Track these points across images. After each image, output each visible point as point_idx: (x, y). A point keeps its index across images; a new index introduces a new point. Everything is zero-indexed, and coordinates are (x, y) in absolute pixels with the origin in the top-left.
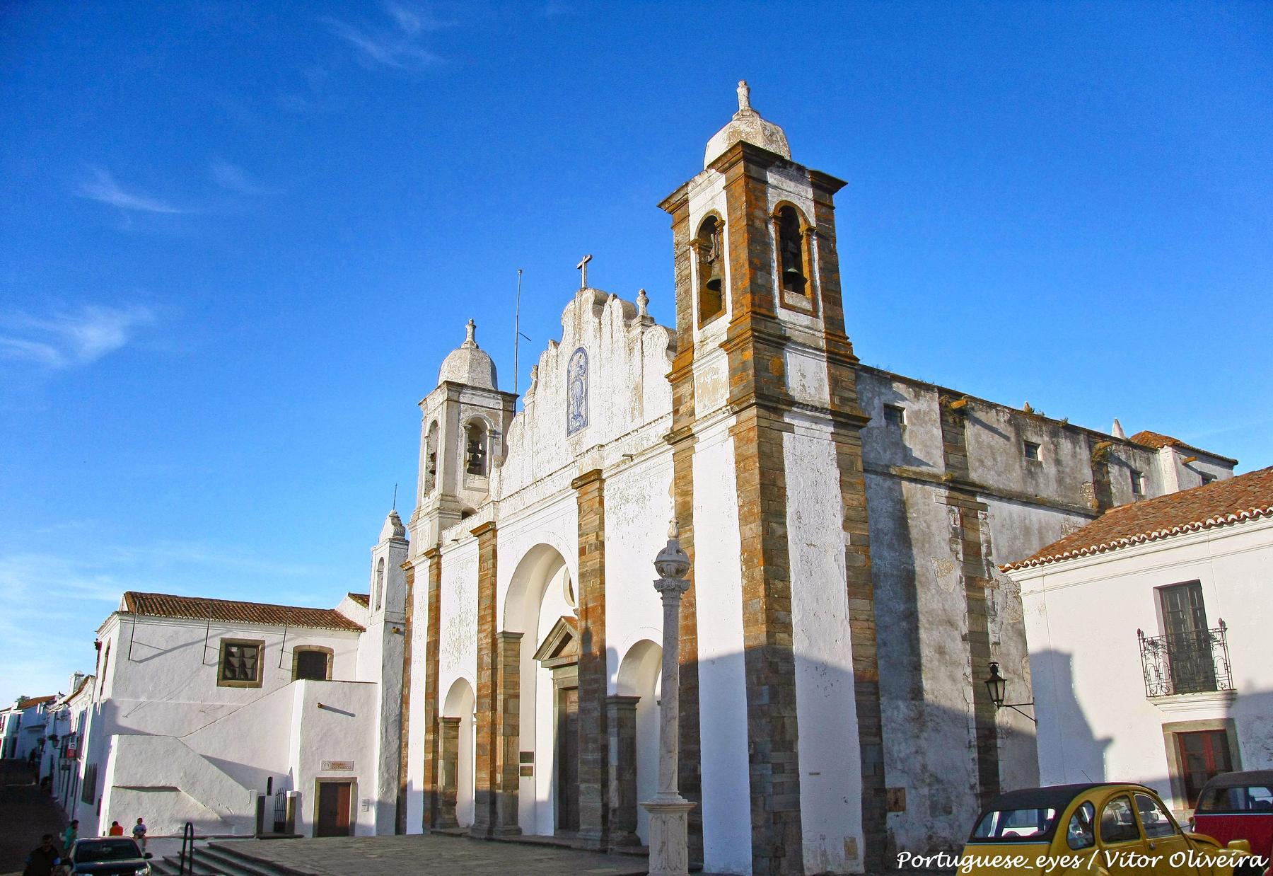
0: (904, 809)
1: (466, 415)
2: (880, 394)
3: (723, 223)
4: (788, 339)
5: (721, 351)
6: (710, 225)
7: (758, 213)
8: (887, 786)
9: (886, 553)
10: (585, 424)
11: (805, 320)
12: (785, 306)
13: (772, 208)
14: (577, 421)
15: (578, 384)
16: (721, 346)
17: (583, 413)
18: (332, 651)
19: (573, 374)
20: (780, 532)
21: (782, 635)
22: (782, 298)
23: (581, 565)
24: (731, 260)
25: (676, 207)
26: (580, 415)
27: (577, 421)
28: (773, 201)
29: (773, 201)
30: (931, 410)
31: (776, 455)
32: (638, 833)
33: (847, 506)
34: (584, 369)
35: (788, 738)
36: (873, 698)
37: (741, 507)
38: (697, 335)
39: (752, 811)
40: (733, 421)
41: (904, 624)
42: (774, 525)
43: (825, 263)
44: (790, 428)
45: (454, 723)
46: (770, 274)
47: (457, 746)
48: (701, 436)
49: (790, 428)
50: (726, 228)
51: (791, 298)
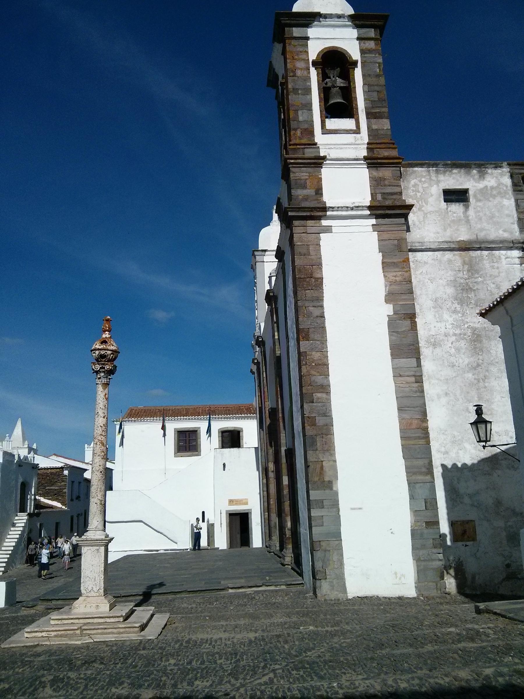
2: (438, 182)
4: (324, 158)
11: (350, 138)
12: (325, 131)
13: (313, 55)
21: (319, 395)
29: (314, 50)
30: (500, 184)
33: (389, 283)
35: (327, 479)
36: (422, 442)
42: (310, 308)
43: (369, 85)
44: (328, 230)
46: (310, 109)
51: (332, 123)
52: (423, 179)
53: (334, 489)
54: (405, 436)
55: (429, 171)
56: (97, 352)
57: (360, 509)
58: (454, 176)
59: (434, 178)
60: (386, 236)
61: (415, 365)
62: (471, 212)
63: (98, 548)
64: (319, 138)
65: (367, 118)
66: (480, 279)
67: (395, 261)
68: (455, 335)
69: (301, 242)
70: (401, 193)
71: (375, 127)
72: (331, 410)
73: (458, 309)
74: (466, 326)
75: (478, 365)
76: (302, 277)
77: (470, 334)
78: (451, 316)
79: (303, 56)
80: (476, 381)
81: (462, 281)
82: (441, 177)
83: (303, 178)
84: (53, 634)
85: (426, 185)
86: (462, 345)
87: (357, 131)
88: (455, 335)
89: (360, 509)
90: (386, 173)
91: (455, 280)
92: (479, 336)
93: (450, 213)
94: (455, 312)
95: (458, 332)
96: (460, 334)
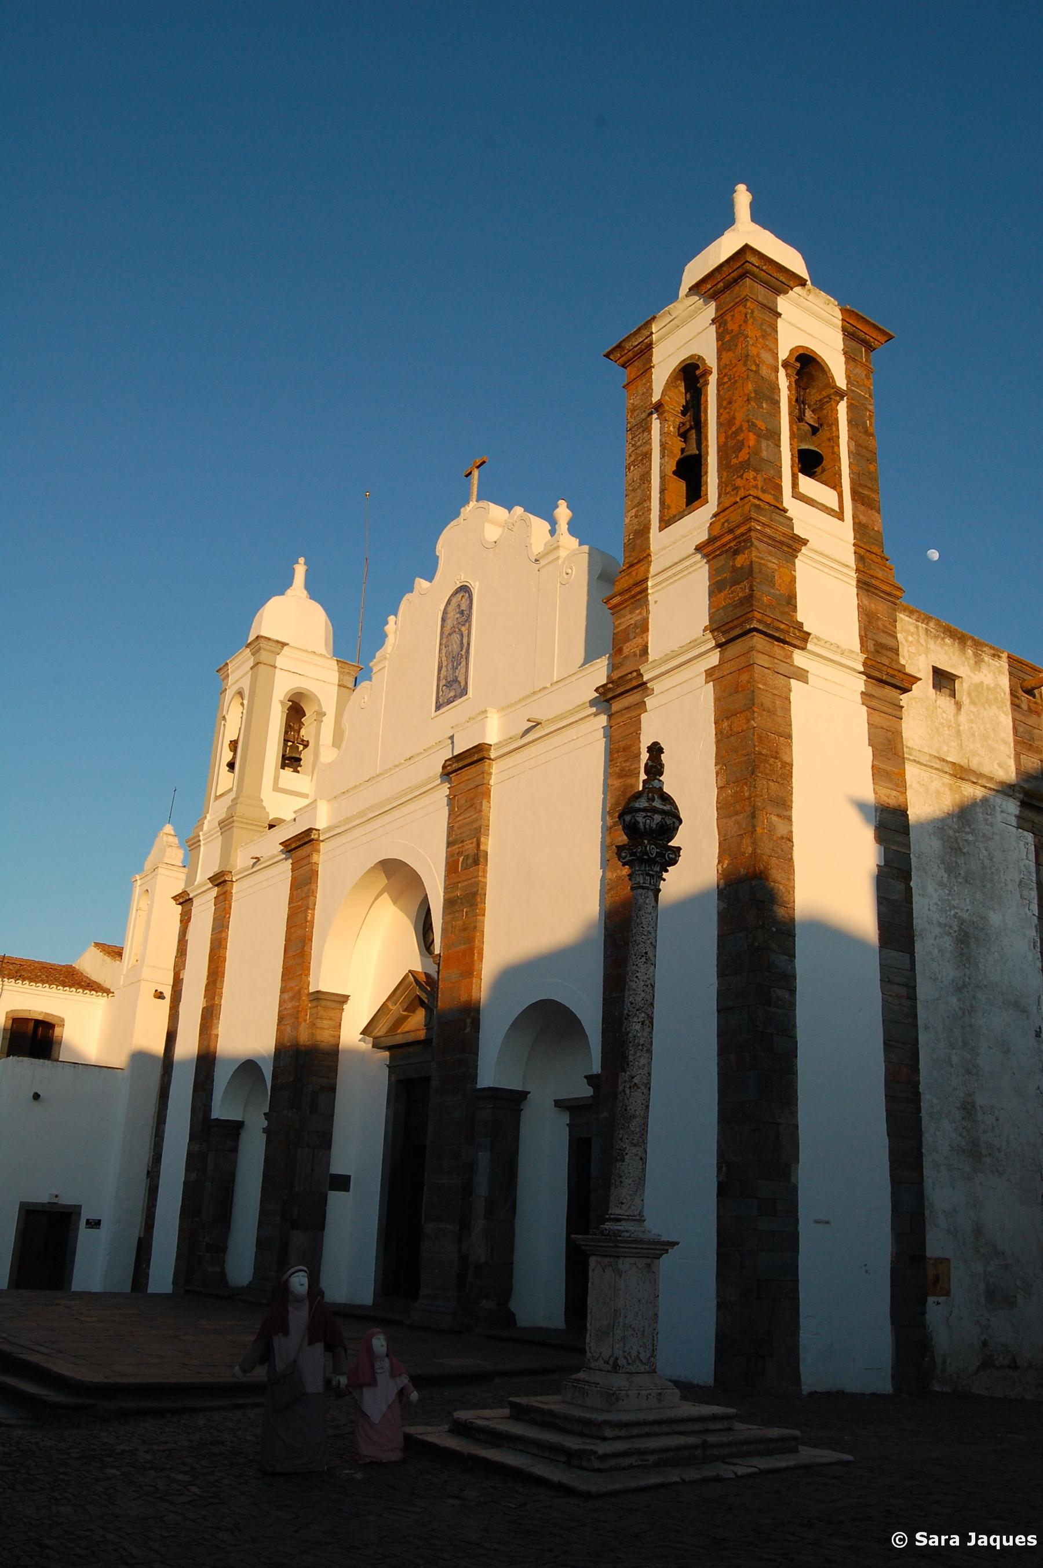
0: (947, 1293)
1: (282, 687)
2: (928, 650)
3: (707, 372)
5: (699, 556)
6: (690, 374)
7: (766, 356)
8: (928, 1254)
9: (930, 888)
10: (464, 692)
12: (797, 495)
13: (783, 354)
14: (452, 686)
15: (456, 637)
16: (698, 549)
17: (461, 679)
18: (63, 1020)
19: (449, 623)
20: (781, 829)
21: (780, 992)
22: (795, 484)
23: (449, 887)
24: (719, 424)
25: (635, 355)
26: (456, 680)
27: (452, 686)
28: (789, 338)
30: (997, 685)
31: (779, 712)
32: (513, 1306)
34: (465, 616)
37: (720, 789)
38: (657, 539)
39: (719, 1275)
40: (714, 658)
41: (954, 1000)
42: (774, 818)
43: (858, 445)
44: (802, 676)
45: (234, 1129)
46: (778, 445)
47: (234, 1163)
48: (657, 686)
49: (802, 676)
50: (713, 379)
51: (808, 485)
52: (910, 638)
53: (793, 1180)
54: (890, 1098)
55: (917, 627)
56: (658, 818)
57: (827, 1222)
58: (946, 648)
59: (923, 642)
60: (878, 719)
61: (908, 966)
62: (963, 718)
63: (649, 1261)
64: (788, 501)
65: (853, 499)
66: (970, 838)
67: (889, 768)
68: (940, 924)
69: (765, 684)
70: (896, 651)
71: (863, 519)
72: (795, 1026)
73: (945, 880)
74: (953, 912)
75: (964, 986)
76: (764, 752)
77: (956, 928)
78: (936, 891)
79: (772, 346)
80: (960, 1013)
81: (951, 832)
82: (932, 645)
83: (770, 565)
84: (652, 1458)
85: (912, 649)
86: (948, 944)
87: (840, 516)
88: (940, 924)
89: (827, 1222)
90: (880, 607)
91: (942, 828)
92: (966, 934)
93: (939, 711)
94: (941, 884)
95: (943, 920)
96: (945, 925)
